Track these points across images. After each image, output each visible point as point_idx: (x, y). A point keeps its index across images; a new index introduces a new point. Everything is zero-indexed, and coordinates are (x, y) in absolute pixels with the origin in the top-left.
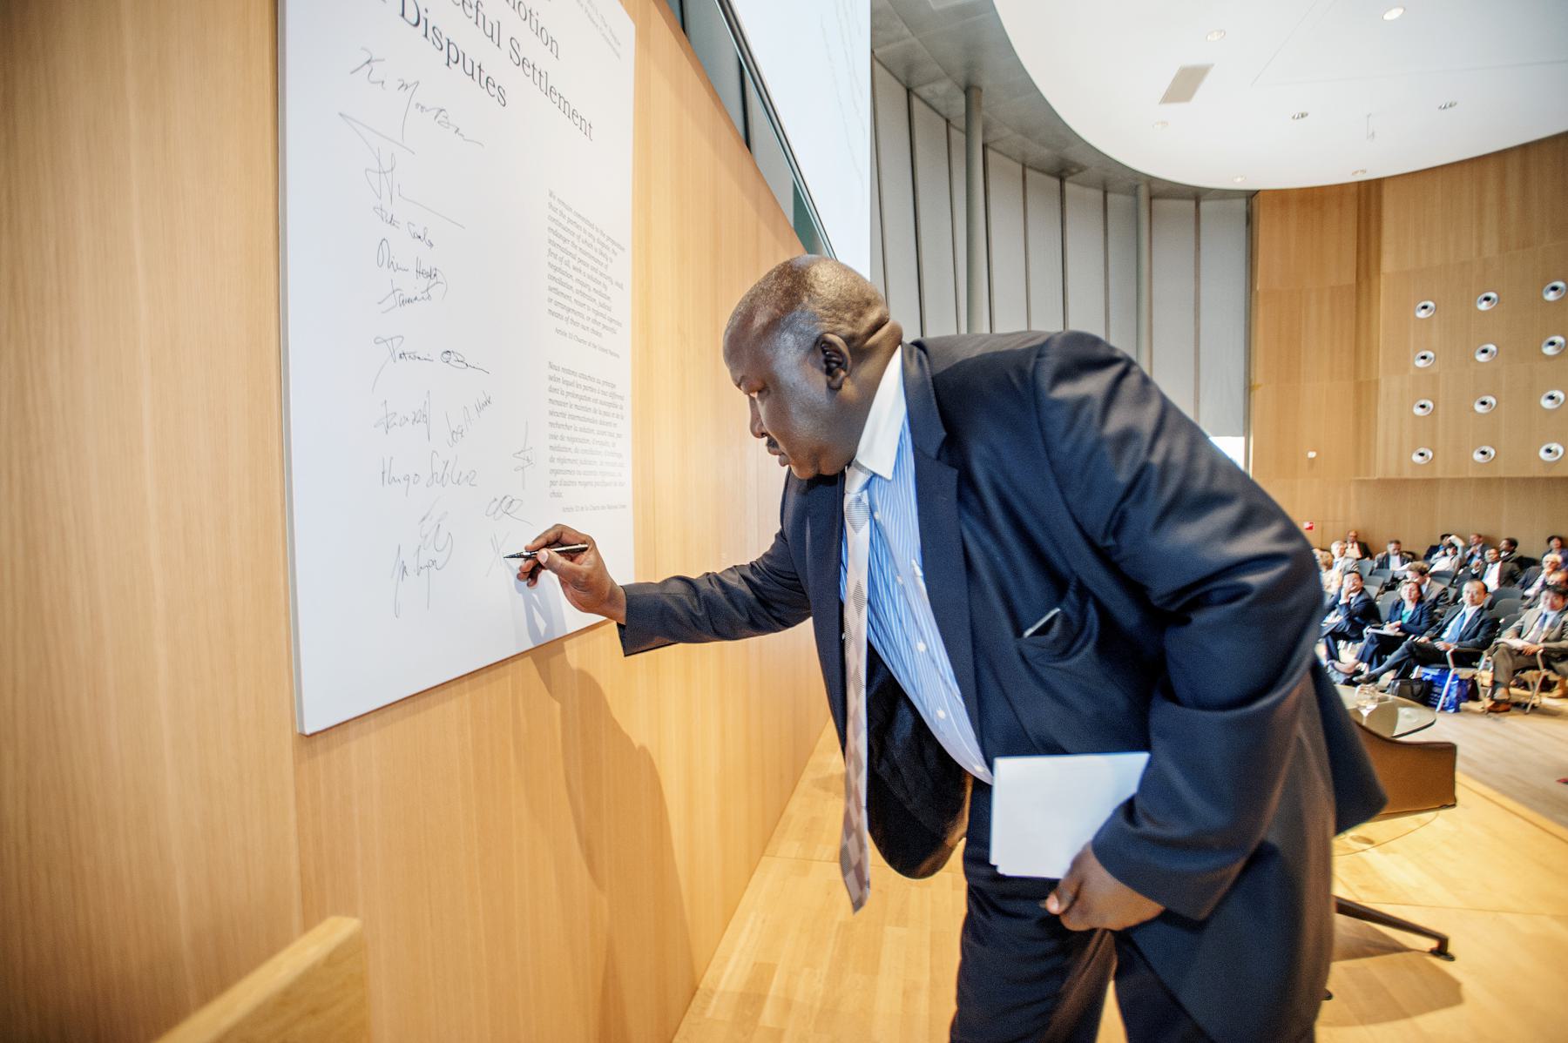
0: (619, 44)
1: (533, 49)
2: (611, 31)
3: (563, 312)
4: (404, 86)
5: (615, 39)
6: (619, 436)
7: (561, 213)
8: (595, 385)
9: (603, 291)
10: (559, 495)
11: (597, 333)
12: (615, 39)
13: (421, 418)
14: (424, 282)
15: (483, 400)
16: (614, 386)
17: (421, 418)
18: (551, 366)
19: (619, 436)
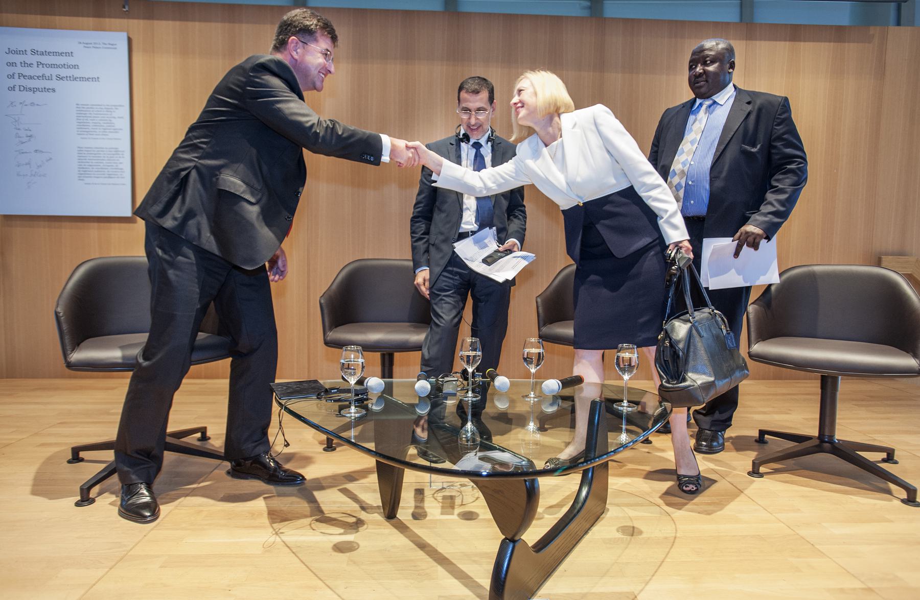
0: (115, 45)
1: (63, 72)
2: (110, 44)
3: (86, 133)
4: (21, 103)
5: (112, 45)
6: (121, 163)
7: (84, 108)
8: (105, 150)
9: (109, 122)
10: (83, 180)
11: (107, 135)
12: (112, 45)
13: (28, 164)
14: (28, 138)
15: (48, 158)
16: (116, 148)
17: (28, 164)
18: (79, 147)
19: (121, 163)
